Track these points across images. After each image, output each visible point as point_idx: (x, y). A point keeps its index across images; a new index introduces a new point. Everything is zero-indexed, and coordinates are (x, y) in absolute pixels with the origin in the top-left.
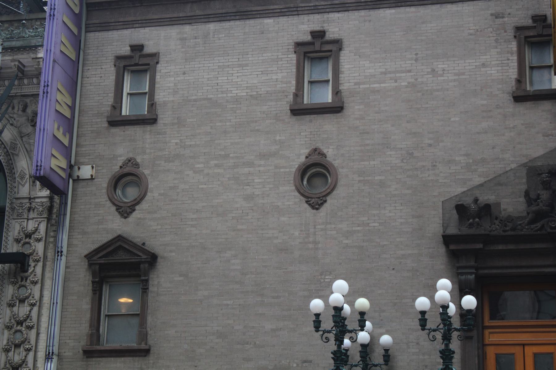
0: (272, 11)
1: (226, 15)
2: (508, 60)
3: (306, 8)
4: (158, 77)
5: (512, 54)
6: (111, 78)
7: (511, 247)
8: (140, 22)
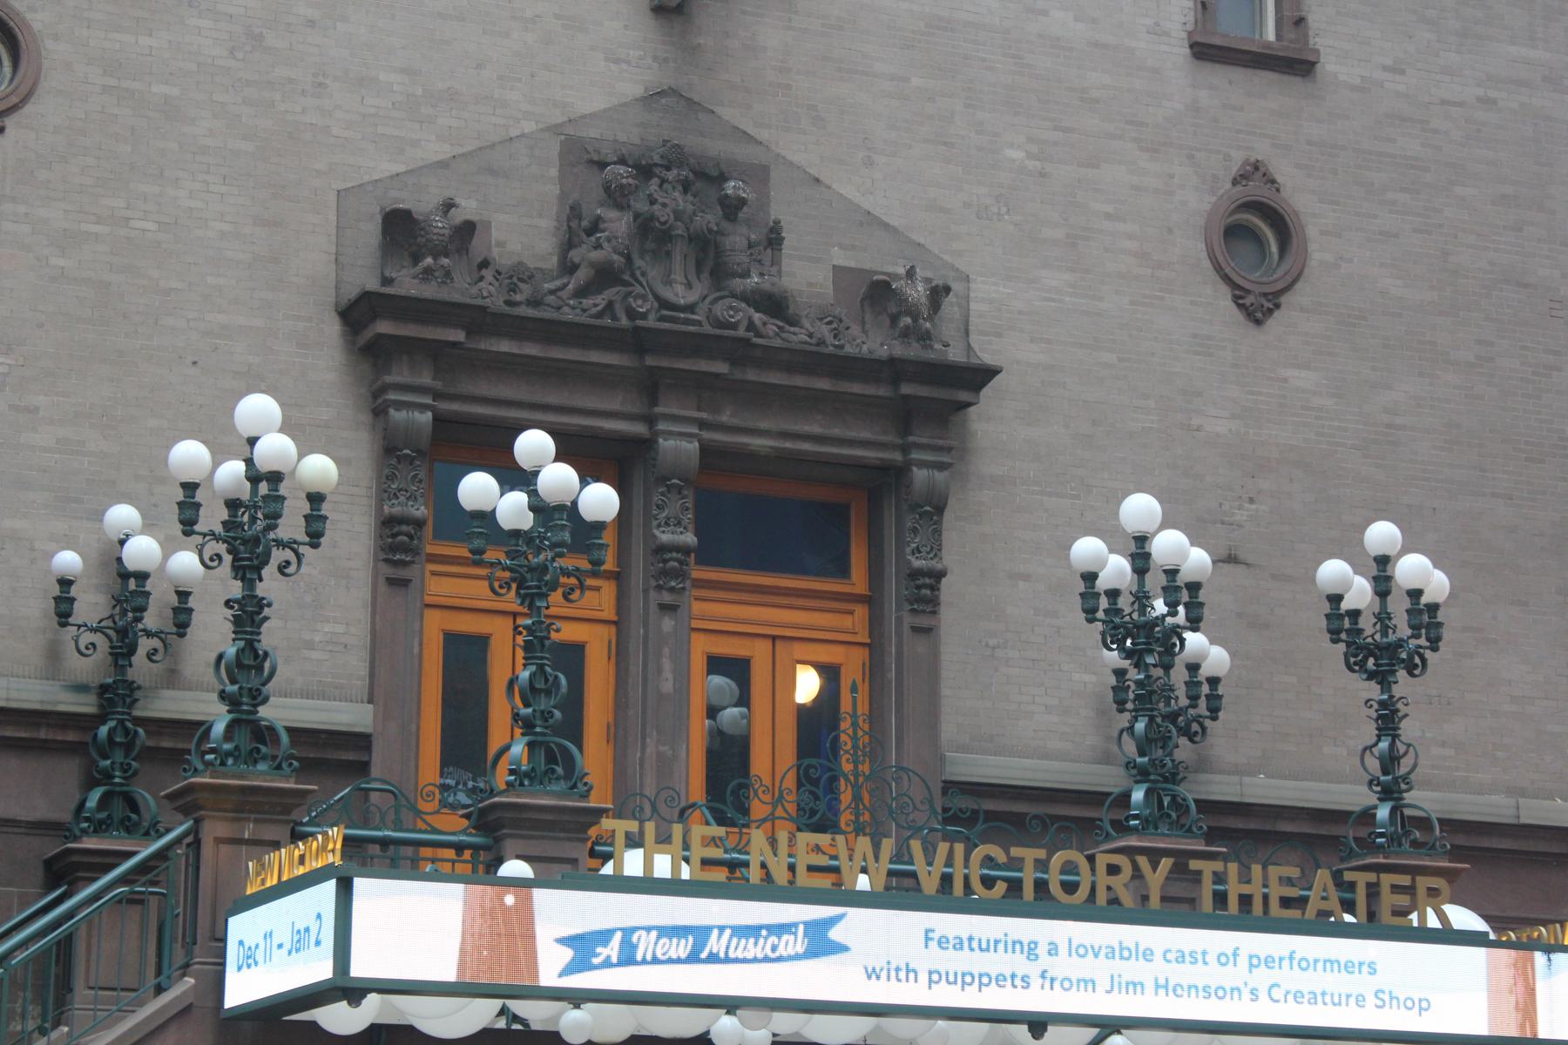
7: (531, 350)
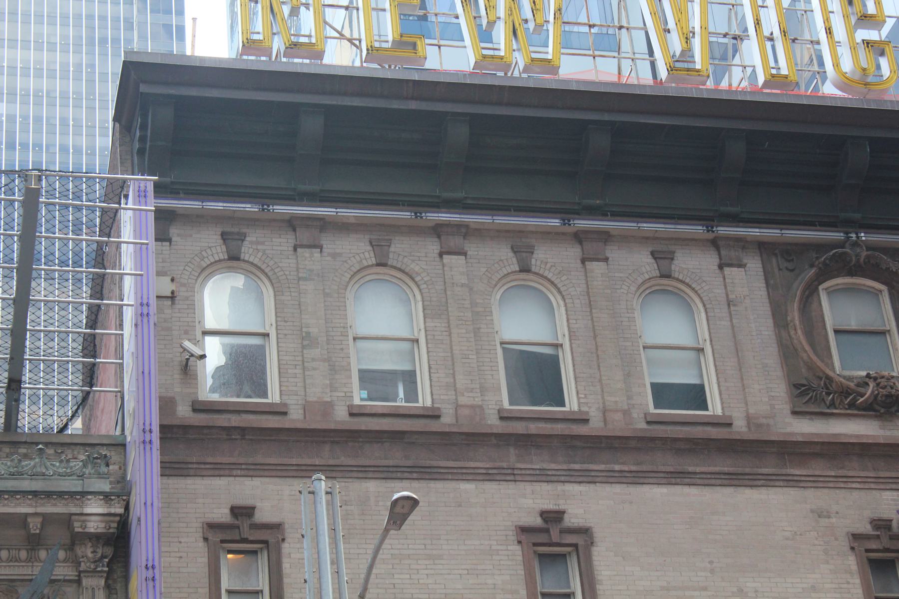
0: (472, 471)
1: (395, 469)
2: (848, 583)
3: (528, 472)
4: (286, 566)
5: (851, 573)
6: (199, 560)
8: (243, 467)
